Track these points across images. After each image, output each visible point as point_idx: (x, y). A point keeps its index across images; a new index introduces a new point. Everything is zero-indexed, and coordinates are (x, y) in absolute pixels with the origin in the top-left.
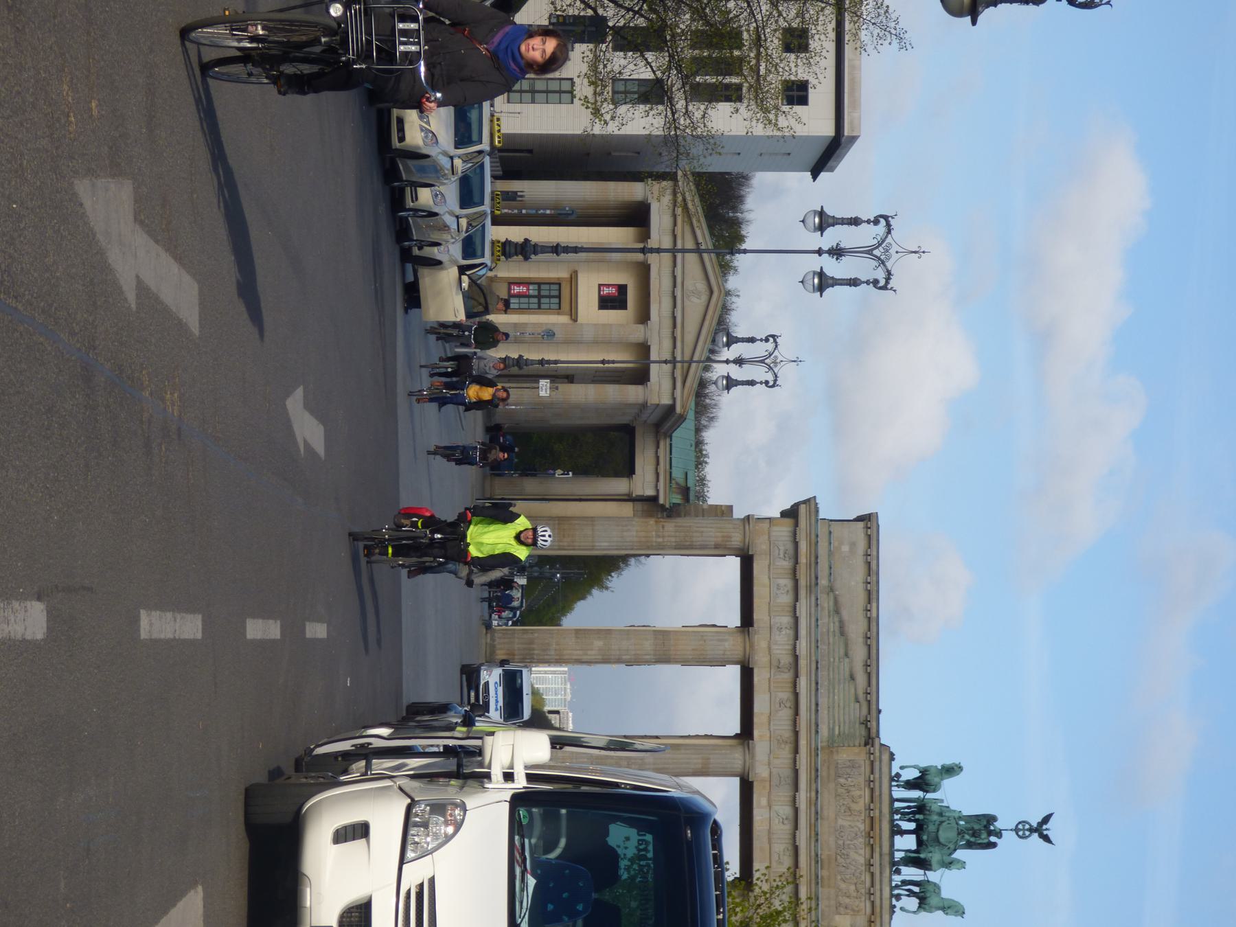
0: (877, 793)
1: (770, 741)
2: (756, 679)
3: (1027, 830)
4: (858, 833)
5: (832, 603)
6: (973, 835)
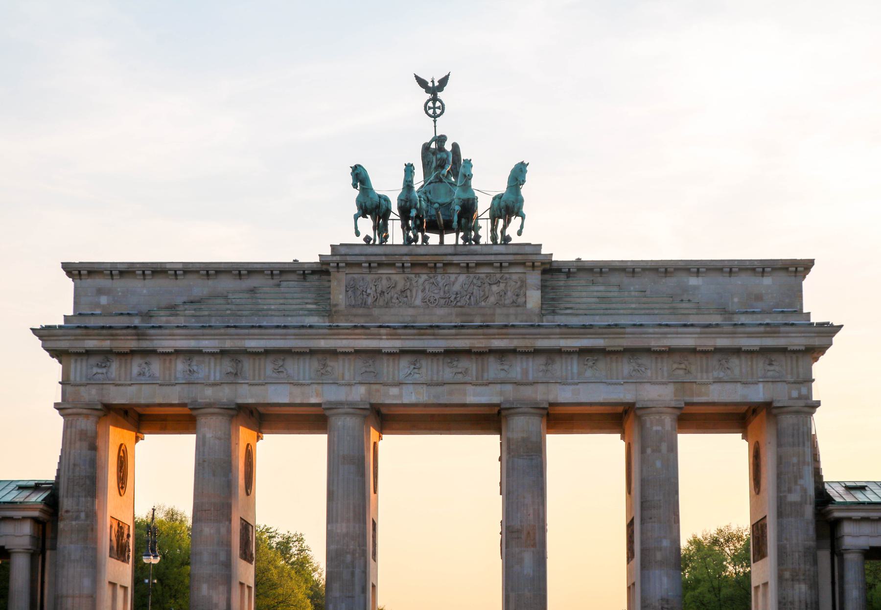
0: (384, 258)
1: (322, 383)
2: (250, 401)
3: (434, 104)
4: (432, 281)
5: (162, 313)
6: (441, 165)
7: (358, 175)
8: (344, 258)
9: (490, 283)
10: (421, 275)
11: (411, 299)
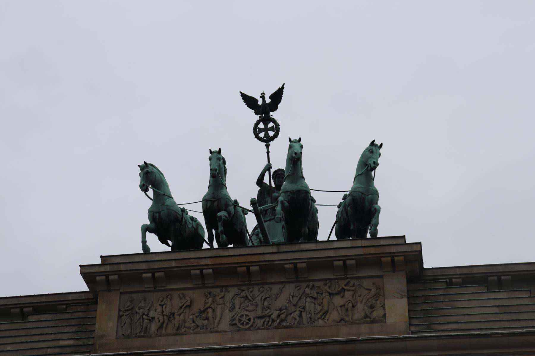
0: (174, 264)
3: (266, 125)
4: (243, 294)
7: (149, 174)
8: (115, 268)
9: (329, 291)
10: (229, 289)
11: (214, 323)
